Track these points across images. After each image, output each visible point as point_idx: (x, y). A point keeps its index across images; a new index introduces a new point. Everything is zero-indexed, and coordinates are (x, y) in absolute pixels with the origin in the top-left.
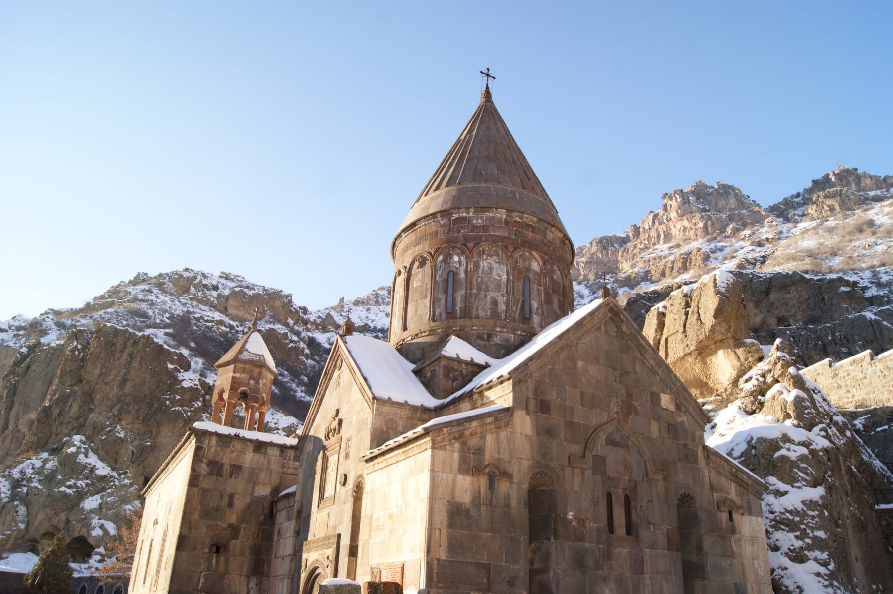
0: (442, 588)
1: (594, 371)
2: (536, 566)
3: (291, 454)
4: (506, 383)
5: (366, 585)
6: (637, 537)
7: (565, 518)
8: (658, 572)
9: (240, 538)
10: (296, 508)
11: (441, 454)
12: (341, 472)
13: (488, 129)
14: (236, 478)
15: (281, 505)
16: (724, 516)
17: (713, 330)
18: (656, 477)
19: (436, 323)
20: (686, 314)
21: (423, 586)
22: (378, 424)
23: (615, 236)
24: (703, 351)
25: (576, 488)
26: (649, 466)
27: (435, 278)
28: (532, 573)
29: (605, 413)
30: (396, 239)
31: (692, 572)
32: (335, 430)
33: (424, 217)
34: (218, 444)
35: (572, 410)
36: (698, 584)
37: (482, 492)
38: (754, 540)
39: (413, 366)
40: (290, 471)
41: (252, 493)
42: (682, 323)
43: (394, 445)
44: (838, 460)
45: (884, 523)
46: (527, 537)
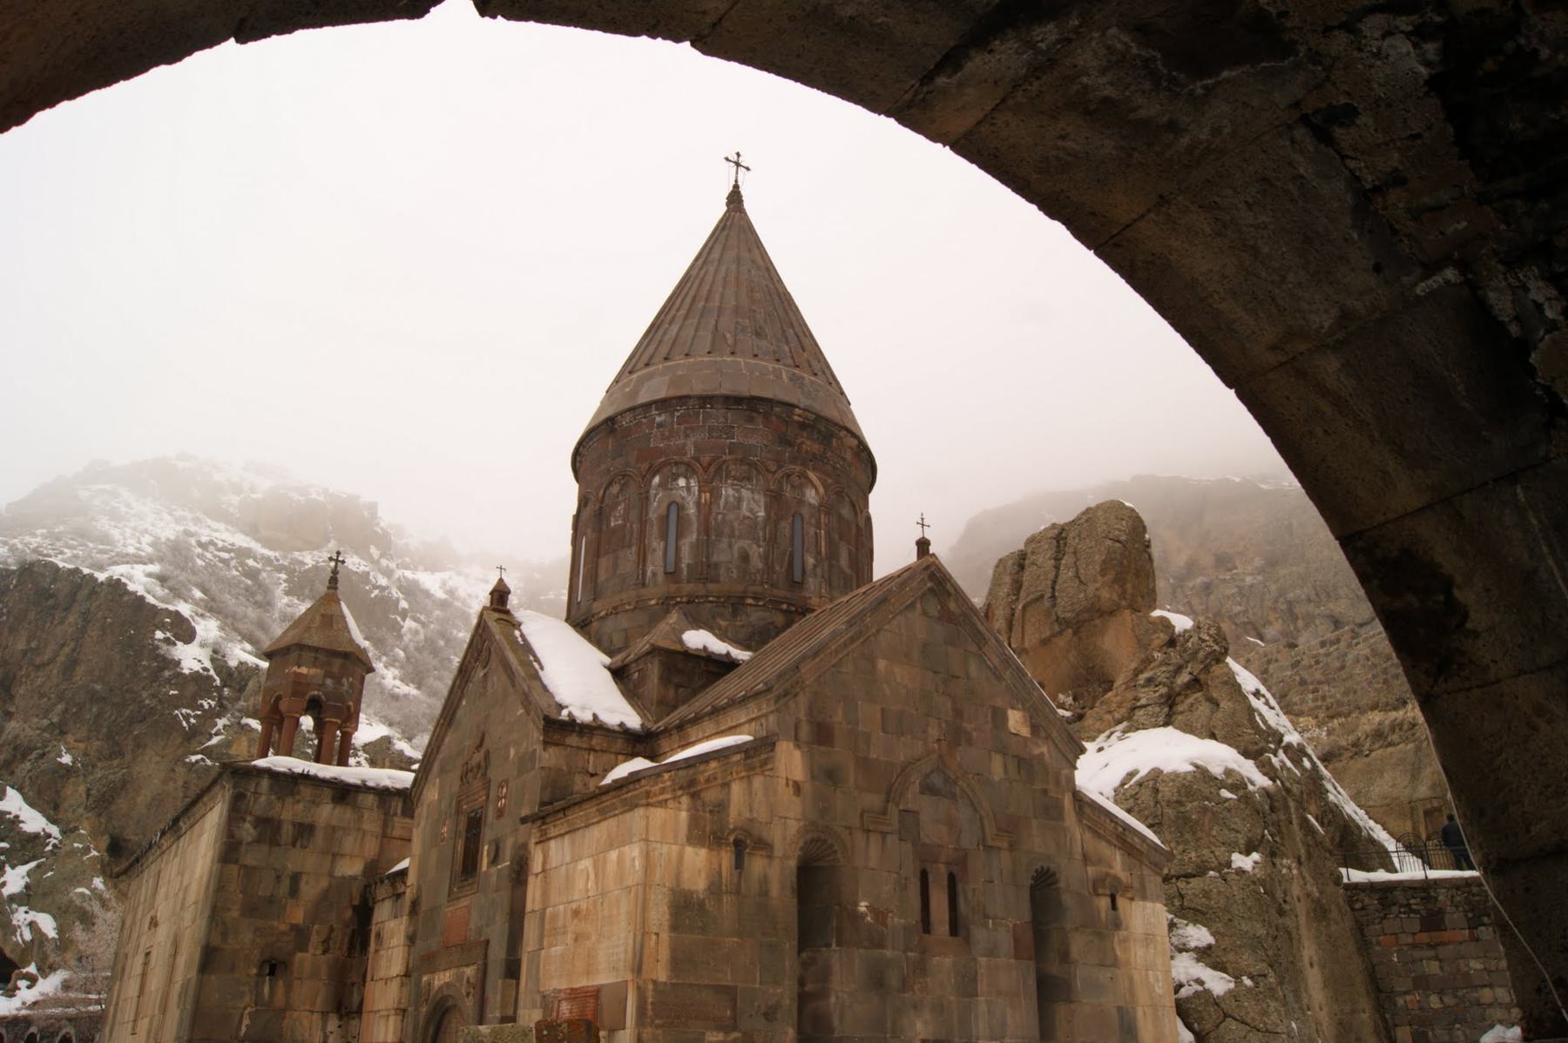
0: (661, 1026)
2: (809, 987)
3: (397, 805)
6: (967, 940)
8: (999, 993)
9: (311, 950)
10: (409, 894)
14: (304, 847)
16: (1104, 903)
28: (803, 999)
31: (1050, 991)
32: (479, 766)
34: (271, 789)
36: (1061, 1011)
38: (1149, 939)
39: (607, 660)
41: (331, 875)
44: (1287, 807)
45: (1358, 906)
46: (795, 943)
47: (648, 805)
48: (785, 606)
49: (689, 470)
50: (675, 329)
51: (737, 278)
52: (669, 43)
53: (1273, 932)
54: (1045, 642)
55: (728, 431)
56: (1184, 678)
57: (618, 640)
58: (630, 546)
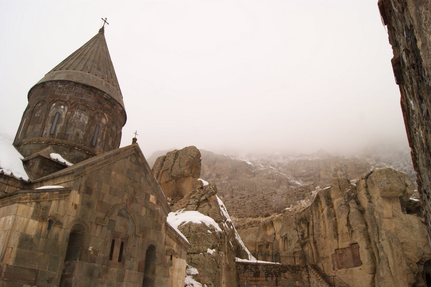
4: (70, 176)
6: (124, 264)
16: (168, 258)
20: (174, 162)
35: (104, 195)
37: (43, 230)
38: (180, 270)
39: (23, 158)
44: (225, 238)
45: (238, 268)
47: (19, 203)
48: (87, 152)
49: (66, 104)
50: (72, 61)
51: (96, 52)
53: (215, 272)
54: (167, 182)
55: (82, 95)
56: (203, 198)
57: (28, 152)
58: (40, 123)
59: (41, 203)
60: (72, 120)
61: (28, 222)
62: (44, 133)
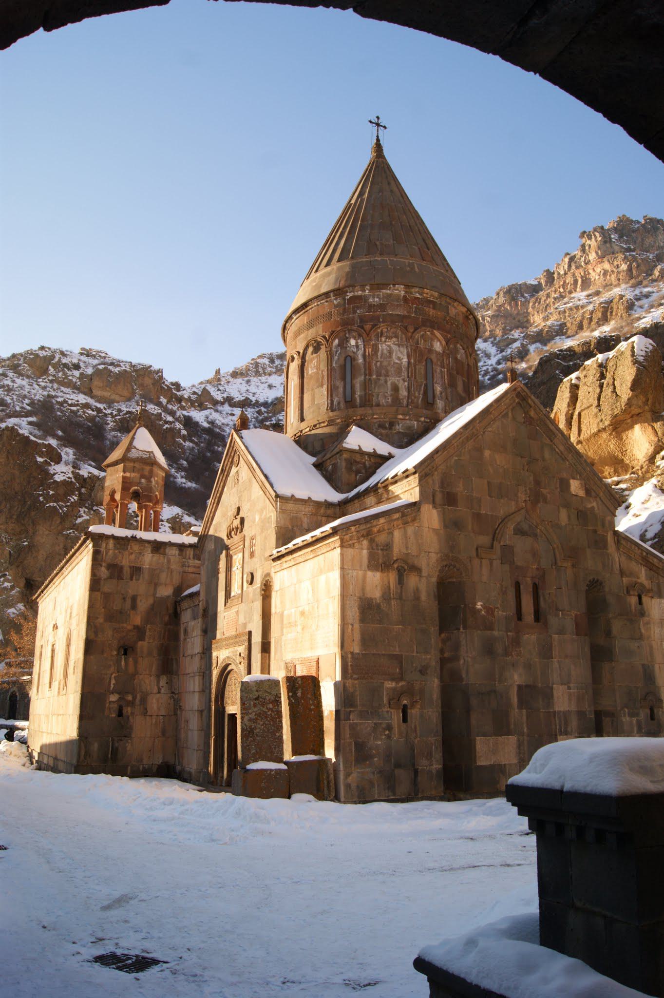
1: (501, 460)
2: (446, 655)
3: (190, 552)
4: (412, 478)
5: (285, 680)
6: (546, 625)
7: (474, 608)
8: (566, 657)
9: (147, 640)
11: (350, 552)
12: (247, 570)
13: (381, 191)
14: (138, 580)
15: (185, 605)
16: (634, 600)
17: (629, 403)
18: (565, 565)
19: (335, 413)
20: (601, 386)
21: (338, 678)
22: (282, 522)
23: (525, 284)
24: (619, 426)
25: (485, 578)
26: (557, 553)
27: (331, 365)
28: (443, 661)
29: (513, 503)
30: (286, 322)
31: (600, 655)
32: (237, 528)
33: (316, 298)
40: (191, 570)
41: (154, 594)
42: (596, 396)
43: (301, 544)
52: (338, 10)
59: (376, 539)
60: (378, 364)
61: (365, 577)
62: (335, 403)
